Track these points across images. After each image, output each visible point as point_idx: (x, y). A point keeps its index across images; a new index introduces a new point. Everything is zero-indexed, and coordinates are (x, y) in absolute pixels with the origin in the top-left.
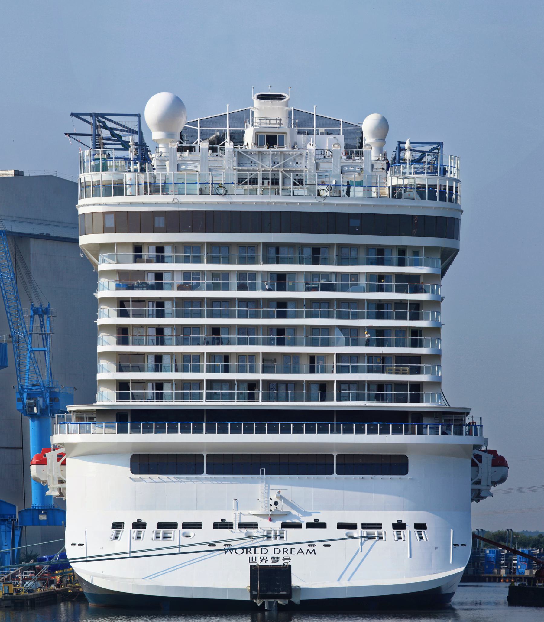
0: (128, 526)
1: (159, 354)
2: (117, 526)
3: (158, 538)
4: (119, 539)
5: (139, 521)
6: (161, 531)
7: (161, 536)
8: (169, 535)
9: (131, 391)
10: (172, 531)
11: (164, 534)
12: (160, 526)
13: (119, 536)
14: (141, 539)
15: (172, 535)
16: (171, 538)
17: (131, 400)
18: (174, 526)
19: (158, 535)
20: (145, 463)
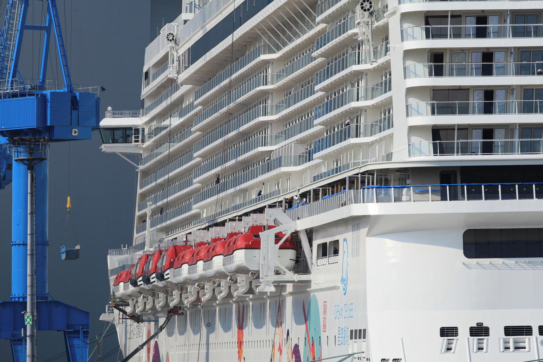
0: (464, 332)
1: (490, 89)
2: (448, 332)
3: (507, 348)
4: (452, 351)
5: (480, 325)
6: (511, 339)
7: (511, 345)
8: (521, 345)
9: (456, 141)
10: (526, 338)
11: (515, 342)
12: (510, 331)
13: (453, 346)
14: (484, 350)
15: (526, 345)
16: (525, 348)
17: (455, 154)
18: (526, 331)
19: (507, 345)
20: (482, 243)
